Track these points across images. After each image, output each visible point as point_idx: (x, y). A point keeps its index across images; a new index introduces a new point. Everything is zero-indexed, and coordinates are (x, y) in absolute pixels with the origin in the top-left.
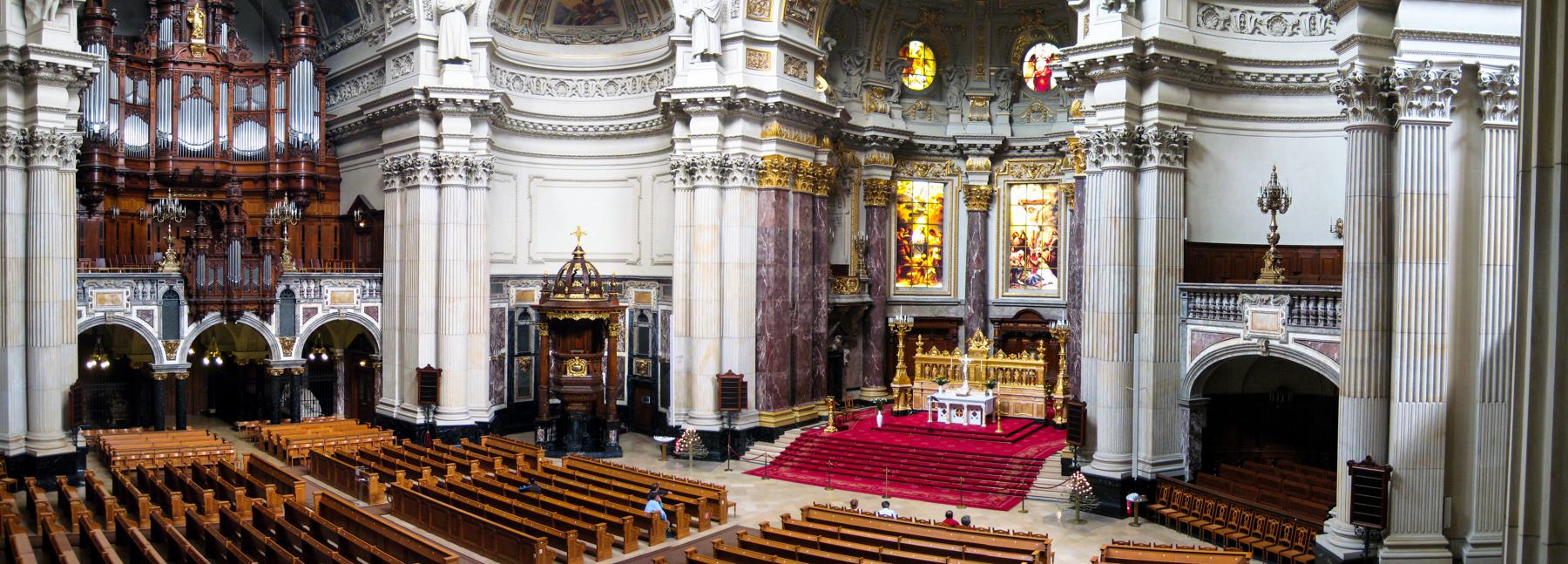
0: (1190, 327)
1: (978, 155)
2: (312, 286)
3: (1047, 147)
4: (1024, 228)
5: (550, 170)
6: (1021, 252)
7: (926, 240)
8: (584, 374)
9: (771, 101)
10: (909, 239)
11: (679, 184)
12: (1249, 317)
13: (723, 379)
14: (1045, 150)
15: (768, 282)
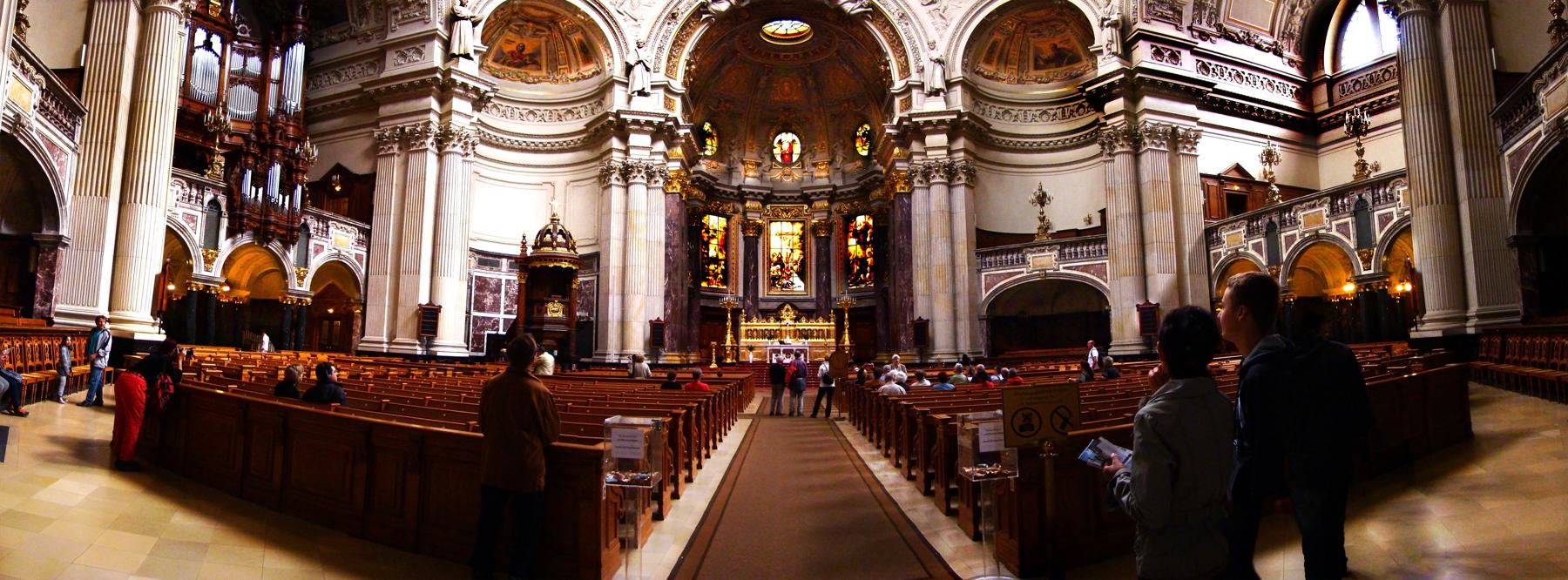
0: (983, 274)
1: (753, 200)
2: (321, 225)
3: (798, 197)
4: (780, 251)
5: (485, 169)
6: (779, 266)
7: (717, 256)
8: (560, 314)
9: (681, 132)
10: (708, 254)
11: (614, 181)
12: (1031, 261)
13: (654, 324)
14: (796, 199)
15: (673, 258)
